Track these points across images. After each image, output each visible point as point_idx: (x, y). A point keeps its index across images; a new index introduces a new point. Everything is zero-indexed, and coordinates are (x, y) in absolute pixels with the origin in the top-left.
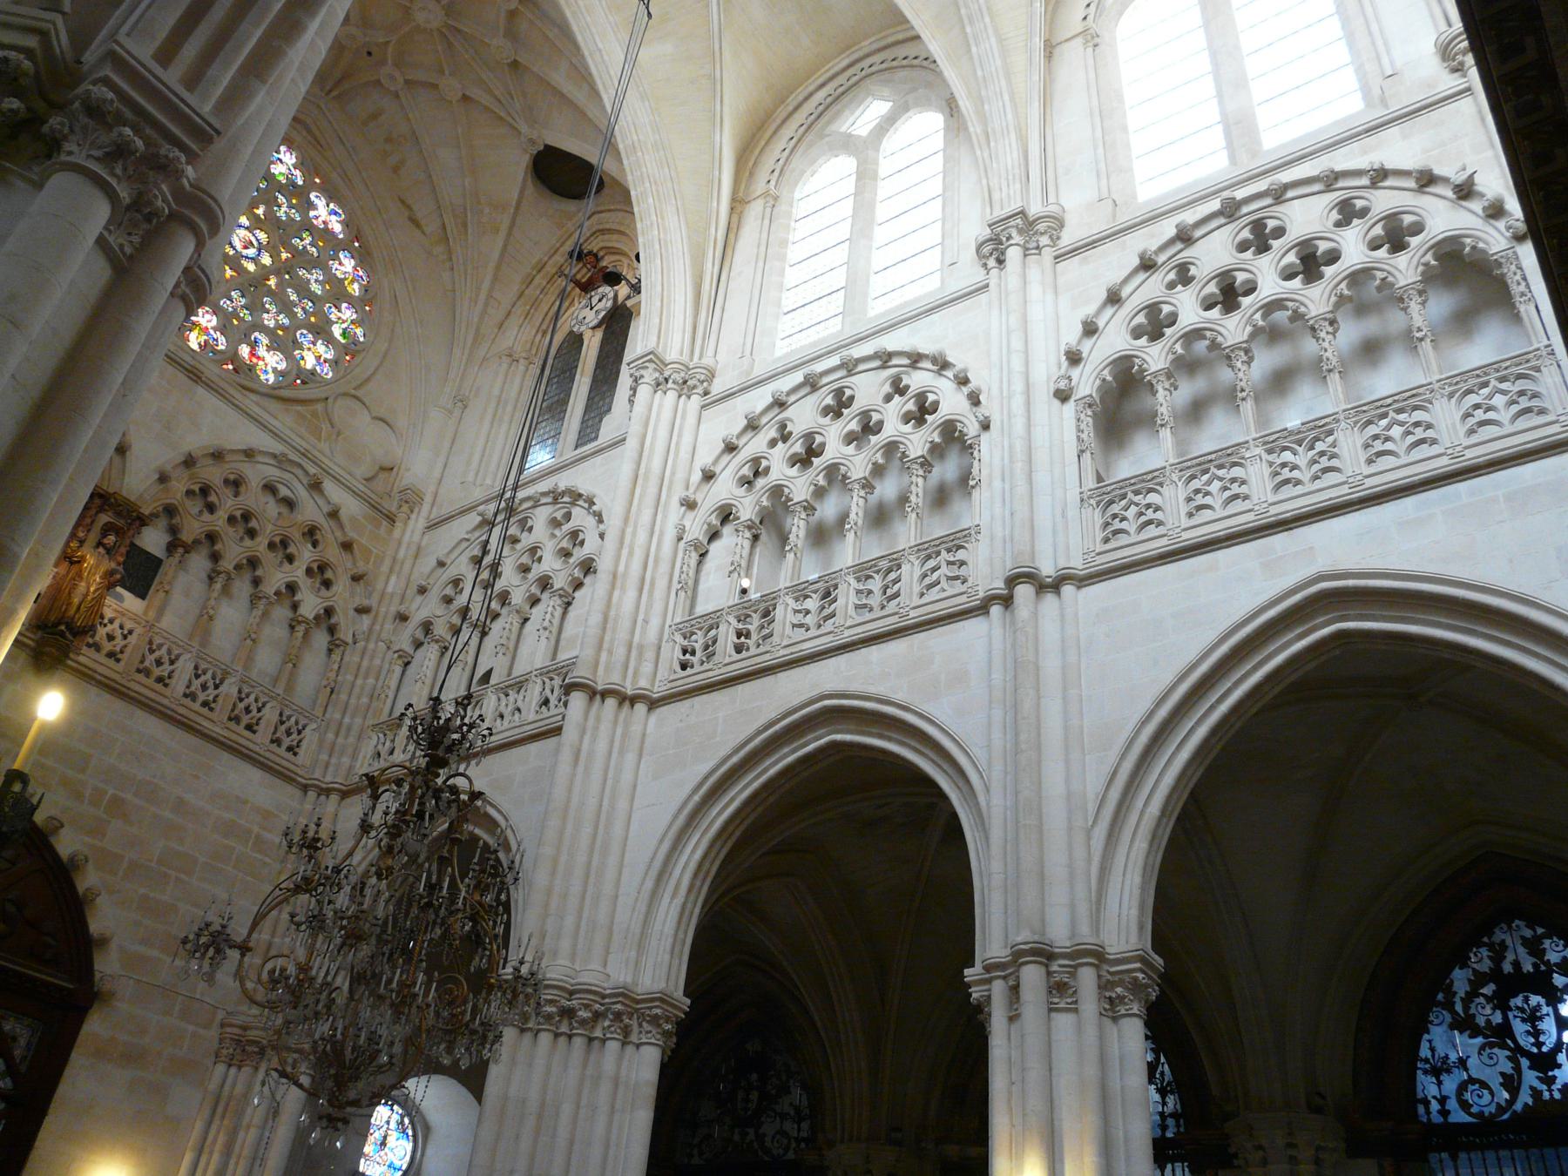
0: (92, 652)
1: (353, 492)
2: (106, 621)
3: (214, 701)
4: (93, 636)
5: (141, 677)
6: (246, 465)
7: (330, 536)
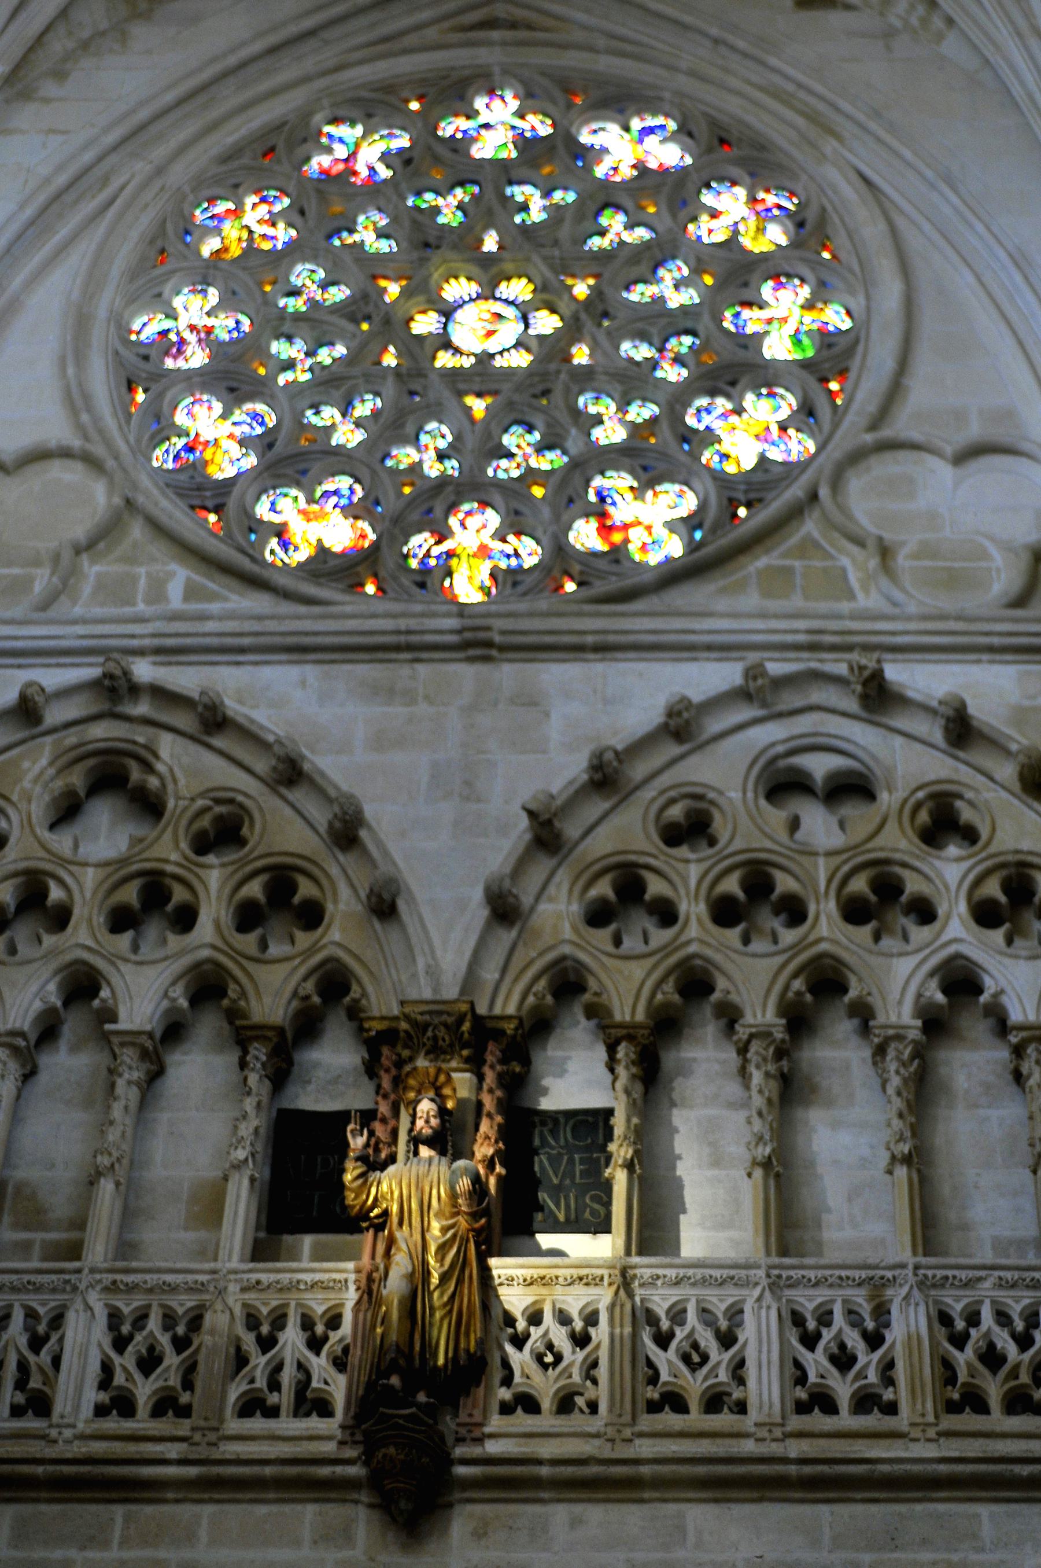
0: (521, 1420)
1: (991, 649)
2: (521, 1325)
3: (889, 1381)
4: (507, 1381)
5: (670, 1419)
6: (694, 760)
7: (991, 794)
